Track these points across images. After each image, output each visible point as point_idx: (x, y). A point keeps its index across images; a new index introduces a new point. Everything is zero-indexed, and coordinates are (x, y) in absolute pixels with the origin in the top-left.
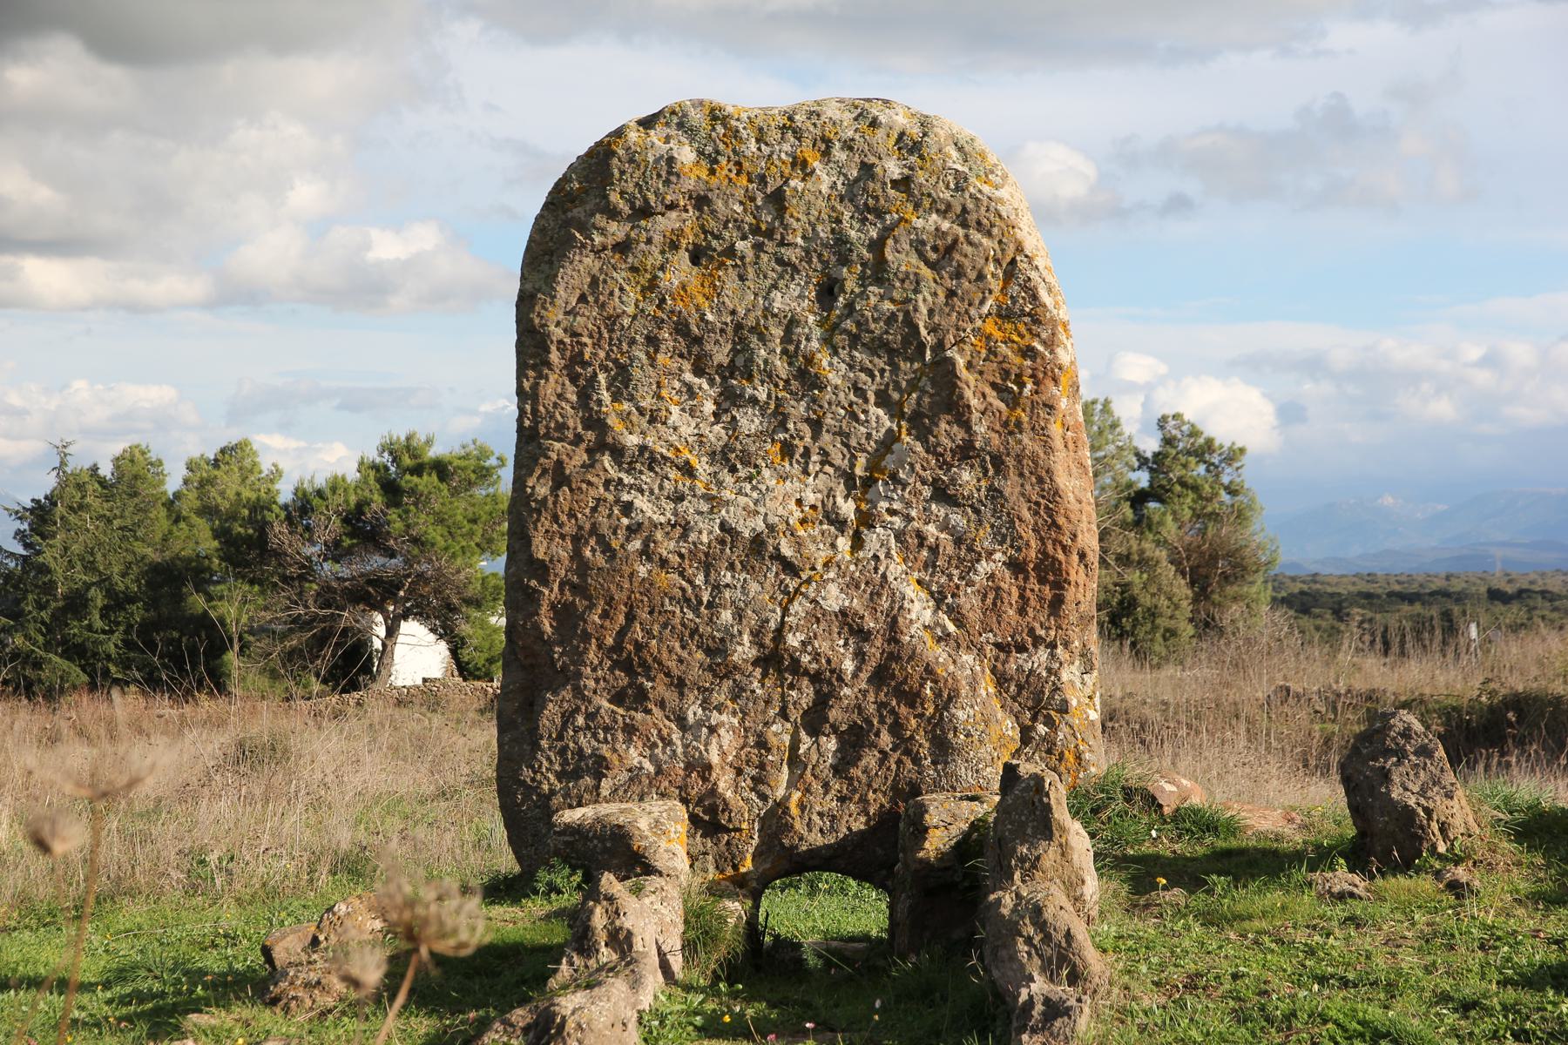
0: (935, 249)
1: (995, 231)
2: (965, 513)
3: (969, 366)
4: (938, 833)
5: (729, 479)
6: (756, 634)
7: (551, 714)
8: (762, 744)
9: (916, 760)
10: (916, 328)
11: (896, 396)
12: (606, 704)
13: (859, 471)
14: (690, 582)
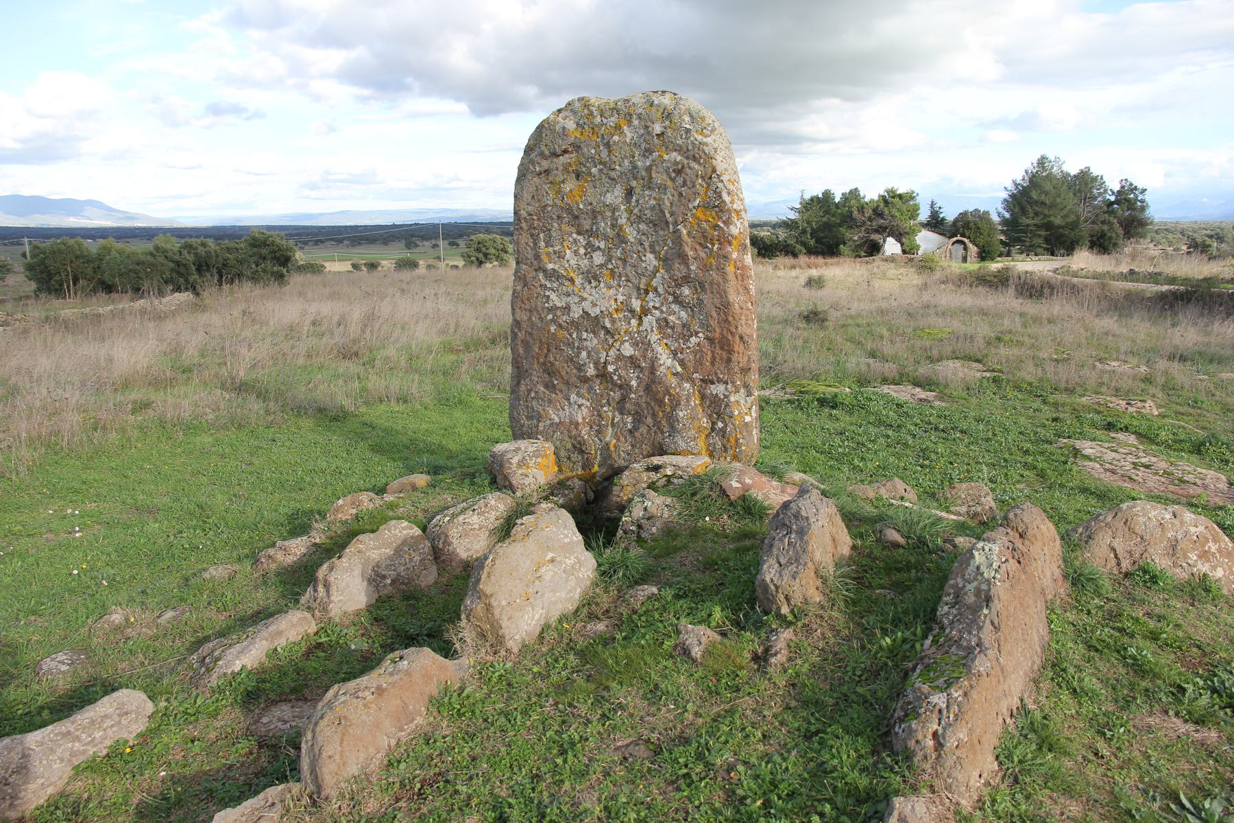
0: (674, 171)
1: (702, 161)
2: (687, 312)
3: (689, 234)
4: (629, 488)
5: (588, 287)
6: (596, 364)
7: (523, 388)
8: (600, 415)
9: (662, 433)
10: (663, 212)
11: (657, 248)
12: (542, 388)
13: (642, 286)
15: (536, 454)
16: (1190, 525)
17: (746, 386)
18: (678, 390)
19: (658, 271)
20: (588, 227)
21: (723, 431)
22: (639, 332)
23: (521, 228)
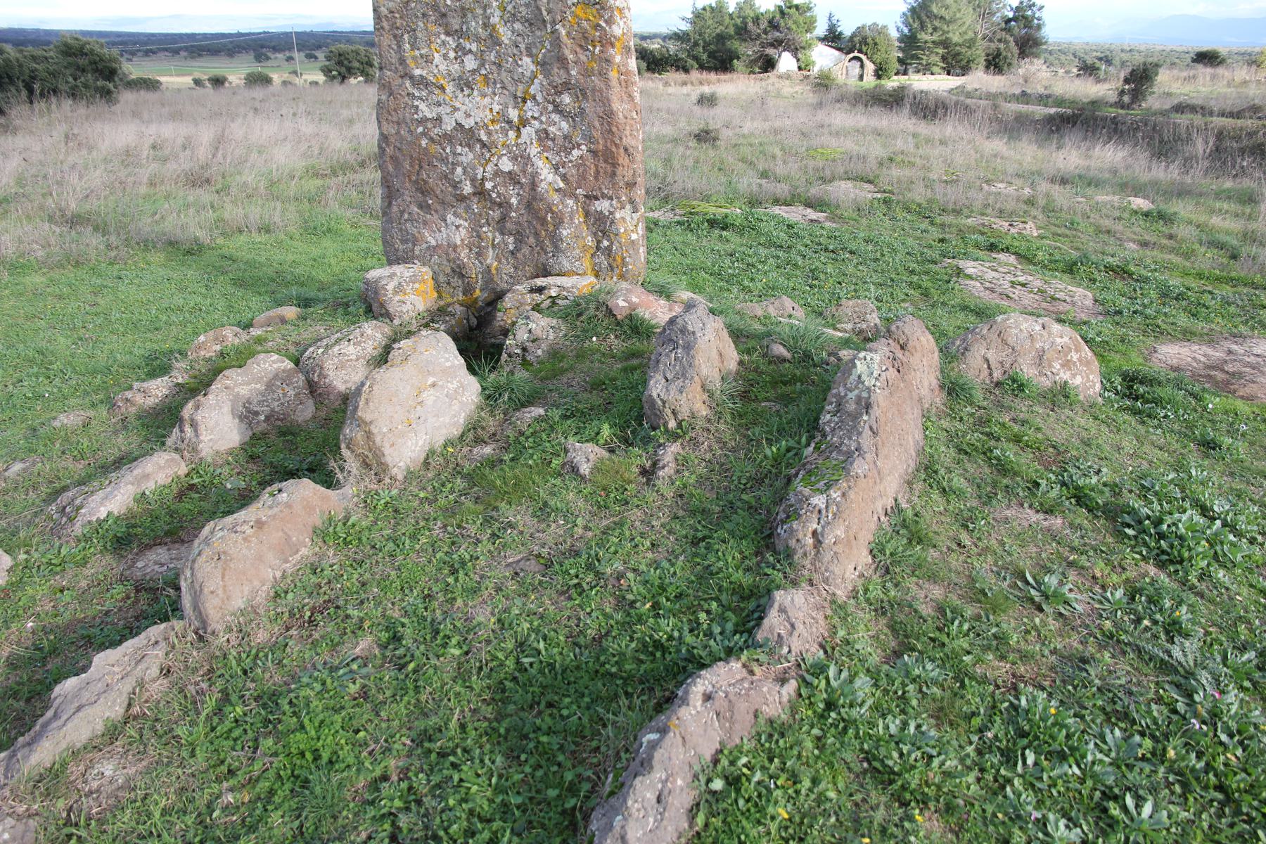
2: (568, 122)
3: (568, 34)
4: (512, 311)
5: (461, 95)
6: (473, 180)
7: (395, 209)
8: (479, 236)
9: (546, 253)
10: (540, 10)
11: (534, 51)
12: (416, 209)
13: (519, 94)
14: (444, 150)
15: (413, 279)
16: (1057, 336)
17: (632, 202)
18: (560, 207)
19: (536, 77)
20: (457, 27)
21: (609, 249)
22: (517, 145)
23: (382, 28)
